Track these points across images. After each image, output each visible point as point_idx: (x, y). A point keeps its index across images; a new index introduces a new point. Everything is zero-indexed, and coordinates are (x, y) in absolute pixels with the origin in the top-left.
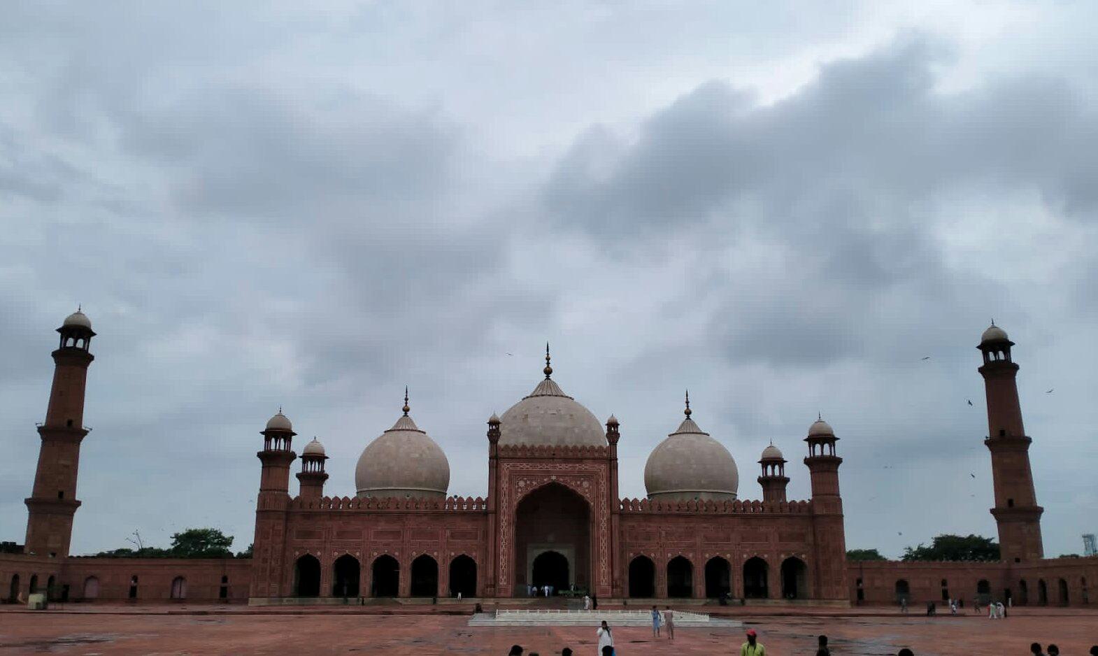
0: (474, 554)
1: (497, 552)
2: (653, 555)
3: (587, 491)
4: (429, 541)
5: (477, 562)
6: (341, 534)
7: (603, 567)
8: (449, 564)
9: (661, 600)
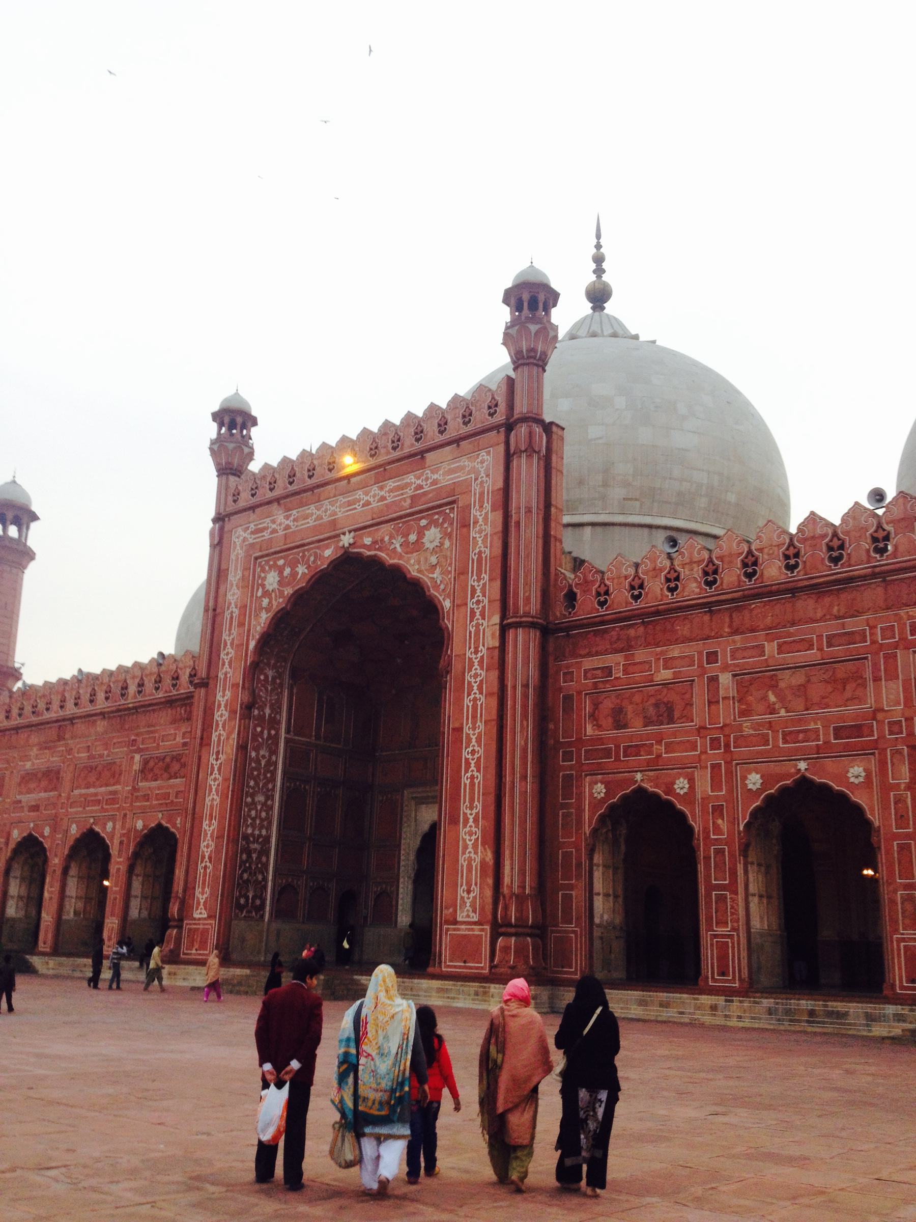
2: (681, 786)
3: (433, 560)
4: (103, 789)
9: (720, 1000)
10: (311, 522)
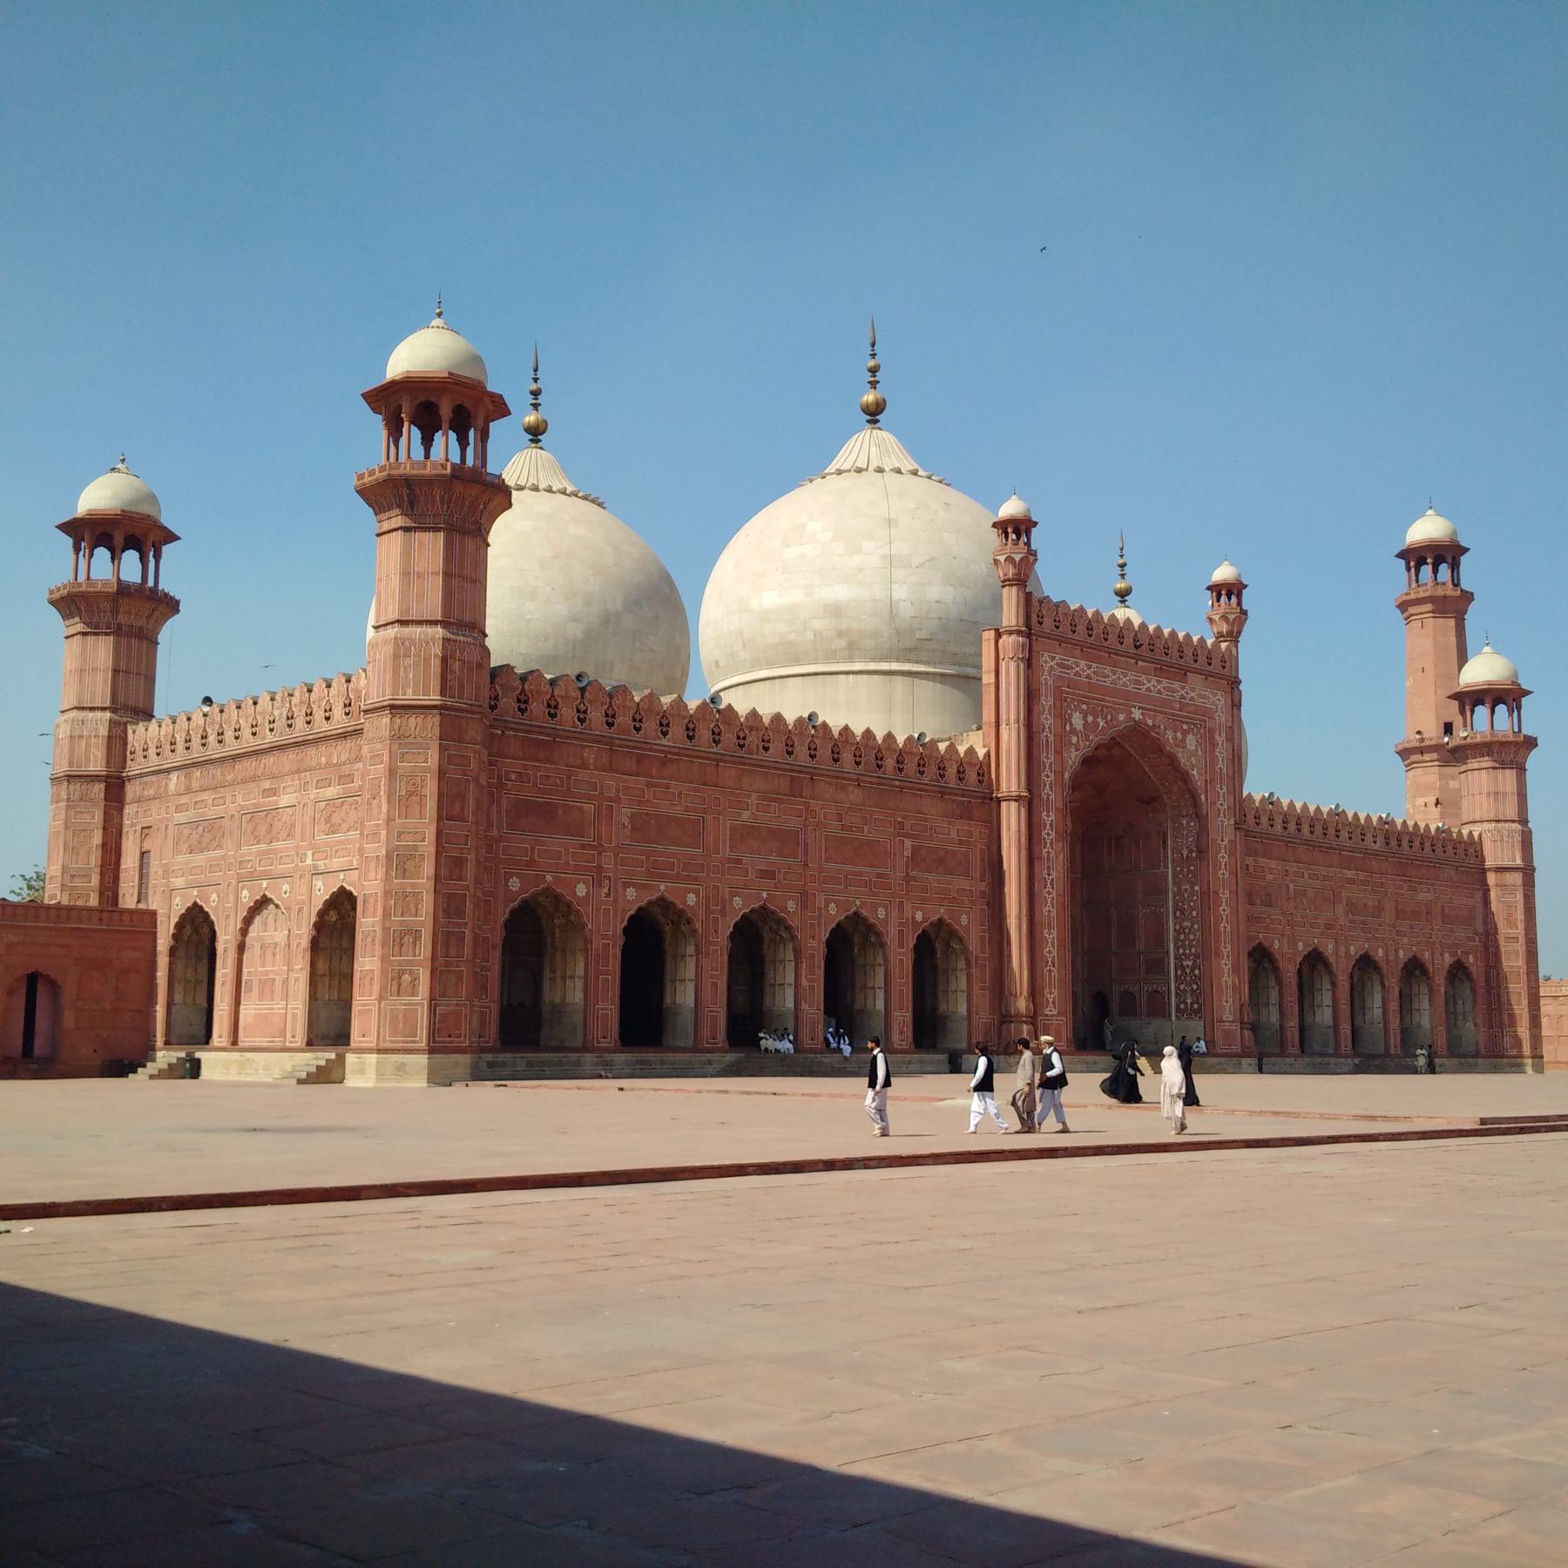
0: (964, 919)
1: (1037, 917)
2: (1276, 945)
4: (864, 869)
5: (973, 945)
6: (639, 824)
7: (1226, 965)
8: (911, 945)
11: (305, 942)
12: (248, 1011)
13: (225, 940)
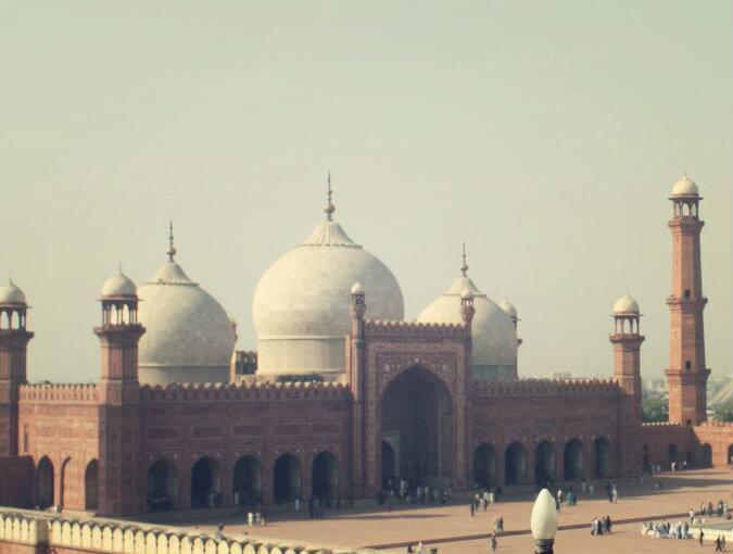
7: (460, 455)
10: (402, 350)
11: (83, 474)
12: (67, 495)
13: (57, 470)
